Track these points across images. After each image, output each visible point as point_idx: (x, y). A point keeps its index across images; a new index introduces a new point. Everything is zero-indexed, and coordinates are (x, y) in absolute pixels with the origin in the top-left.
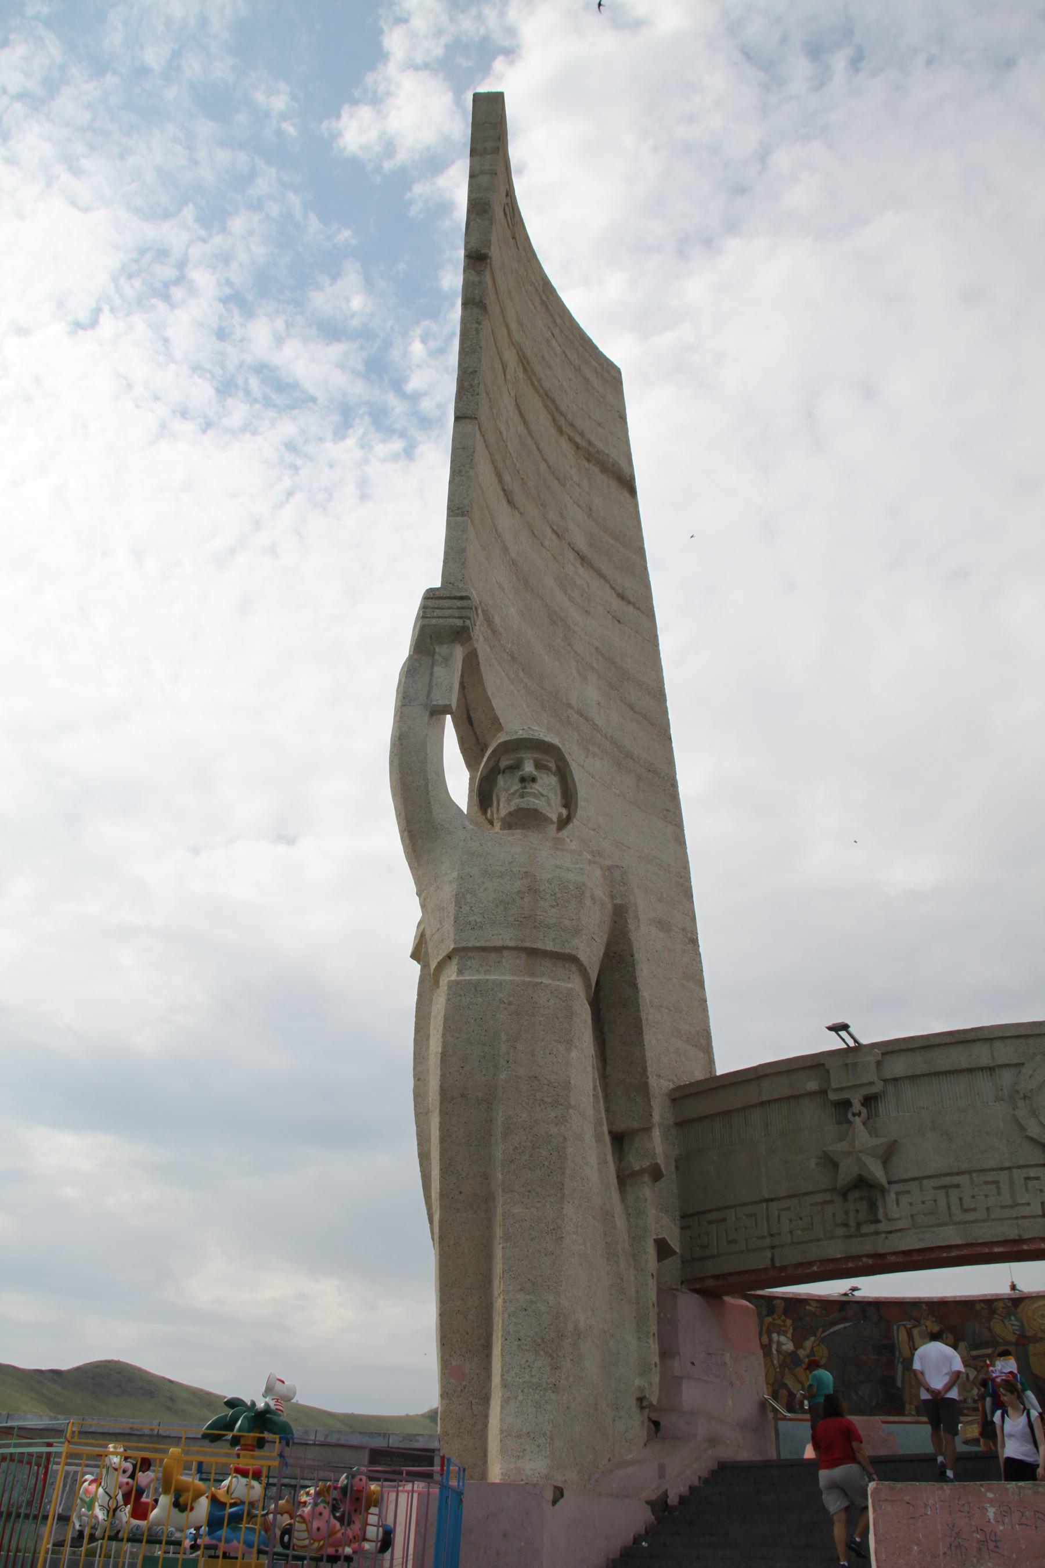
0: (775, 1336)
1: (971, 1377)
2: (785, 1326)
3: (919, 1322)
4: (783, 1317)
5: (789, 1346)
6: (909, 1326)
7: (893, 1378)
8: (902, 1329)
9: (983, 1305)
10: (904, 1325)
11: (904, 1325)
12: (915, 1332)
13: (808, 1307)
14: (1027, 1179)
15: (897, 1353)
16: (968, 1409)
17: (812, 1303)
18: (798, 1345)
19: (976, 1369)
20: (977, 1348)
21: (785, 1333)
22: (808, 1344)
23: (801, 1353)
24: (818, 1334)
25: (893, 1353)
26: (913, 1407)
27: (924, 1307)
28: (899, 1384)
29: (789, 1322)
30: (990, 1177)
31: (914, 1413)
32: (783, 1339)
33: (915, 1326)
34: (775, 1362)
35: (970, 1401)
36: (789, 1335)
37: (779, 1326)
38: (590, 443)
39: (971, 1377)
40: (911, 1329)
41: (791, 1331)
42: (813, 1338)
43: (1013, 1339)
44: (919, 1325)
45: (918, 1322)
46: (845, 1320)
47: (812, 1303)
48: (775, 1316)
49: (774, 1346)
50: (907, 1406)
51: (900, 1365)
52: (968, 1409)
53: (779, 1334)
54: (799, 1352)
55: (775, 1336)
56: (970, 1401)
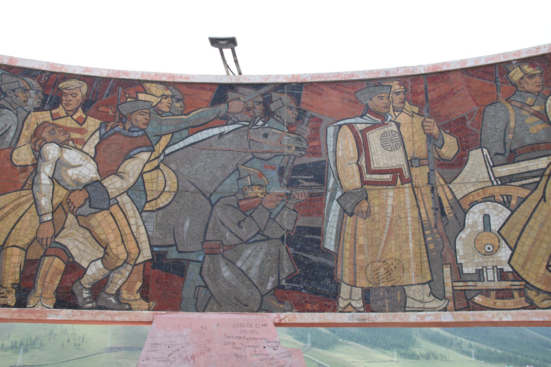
0: (52, 151)
1: (496, 224)
2: (81, 131)
3: (383, 117)
4: (80, 113)
5: (88, 171)
6: (360, 127)
7: (318, 231)
8: (346, 129)
9: (529, 70)
10: (351, 126)
11: (349, 125)
12: (374, 137)
13: (141, 96)
15: (332, 181)
16: (486, 292)
17: (159, 90)
18: (108, 166)
19: (506, 204)
20: (512, 157)
21: (79, 145)
22: (132, 168)
23: (114, 184)
24: (159, 148)
25: (321, 180)
26: (358, 292)
27: (396, 86)
28: (330, 244)
29: (92, 124)
31: (359, 304)
32: (71, 156)
33: (374, 126)
34: (44, 202)
35: (490, 275)
36: (90, 148)
37: (66, 130)
39: (496, 224)
40: (364, 132)
41: (95, 139)
42: (145, 156)
44: (383, 124)
45: (382, 118)
46: (225, 120)
47: (153, 88)
48: (60, 111)
49: (46, 170)
50: (345, 290)
51: (335, 206)
52: (486, 292)
53: (62, 145)
54: (107, 183)
56: (490, 275)
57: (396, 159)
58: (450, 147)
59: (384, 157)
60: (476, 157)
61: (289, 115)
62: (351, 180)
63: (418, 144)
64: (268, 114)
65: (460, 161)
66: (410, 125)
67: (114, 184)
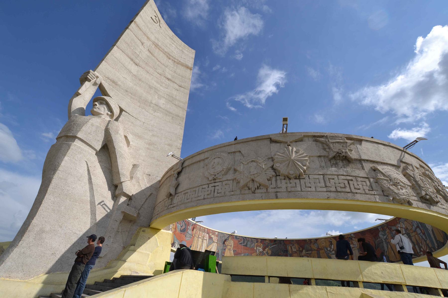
0: (258, 248)
12: (293, 247)
14: (203, 188)
21: (260, 247)
22: (266, 250)
30: (194, 189)
32: (260, 248)
38: (178, 60)
43: (316, 249)
46: (276, 244)
55: (258, 248)
57: (295, 250)
58: (301, 249)
59: (294, 250)
60: (304, 251)
61: (283, 244)
62: (291, 252)
63: (298, 249)
64: (280, 244)
65: (302, 251)
66: (296, 245)
67: (265, 252)
